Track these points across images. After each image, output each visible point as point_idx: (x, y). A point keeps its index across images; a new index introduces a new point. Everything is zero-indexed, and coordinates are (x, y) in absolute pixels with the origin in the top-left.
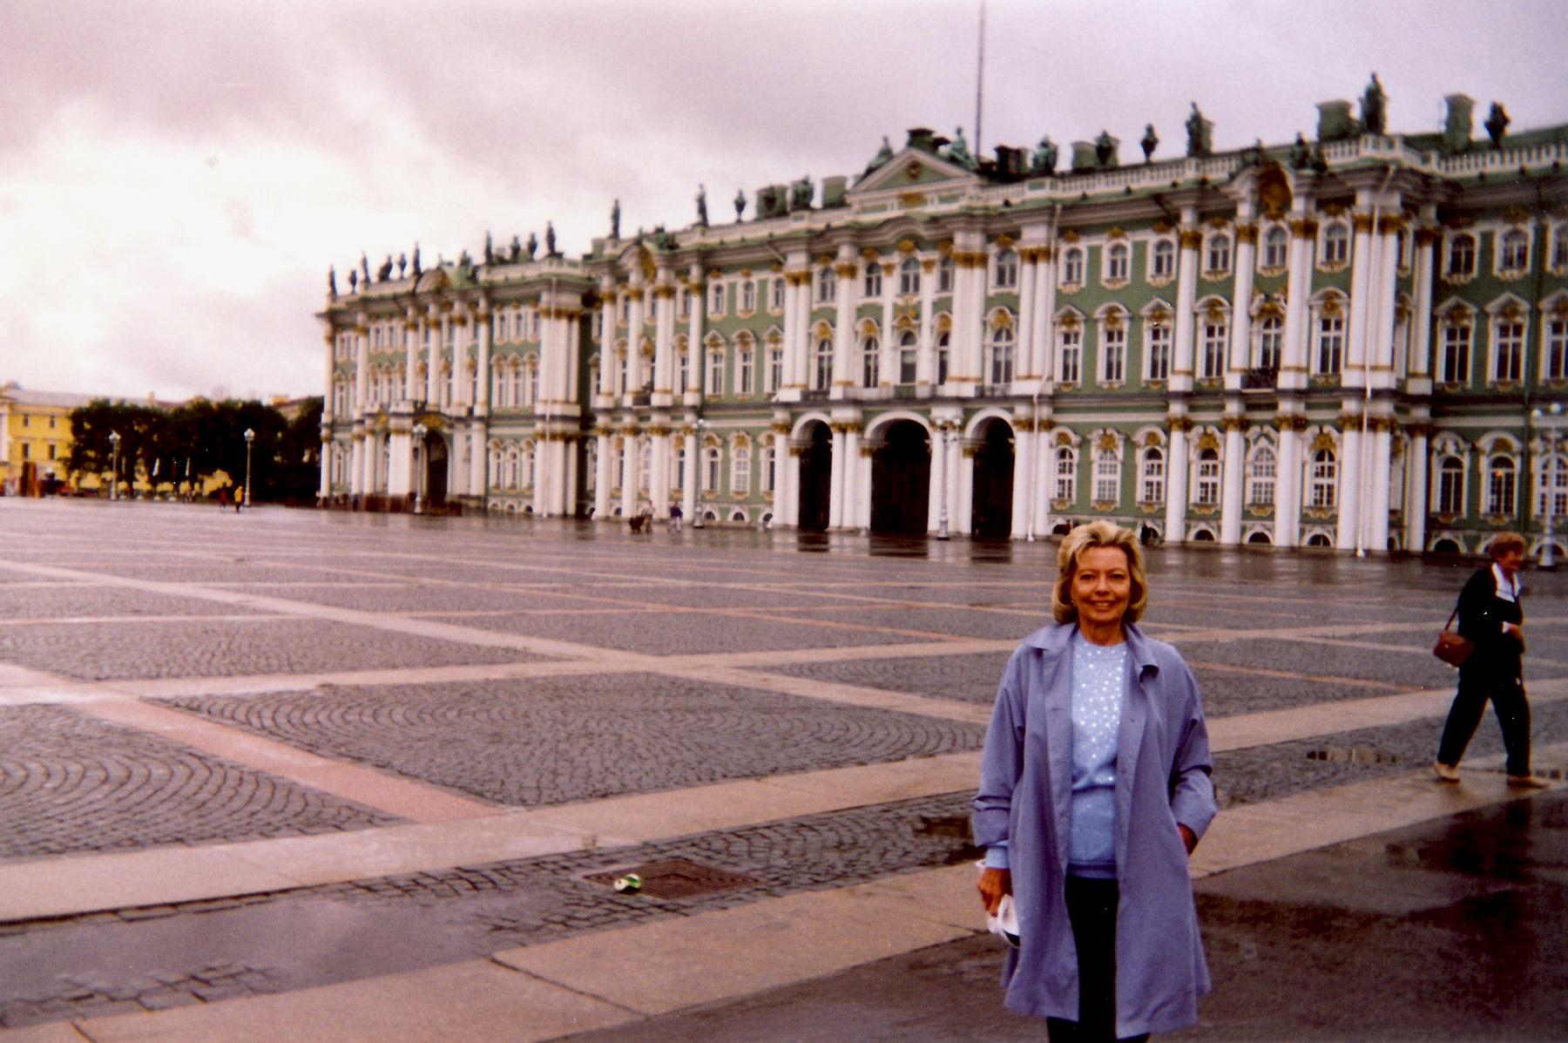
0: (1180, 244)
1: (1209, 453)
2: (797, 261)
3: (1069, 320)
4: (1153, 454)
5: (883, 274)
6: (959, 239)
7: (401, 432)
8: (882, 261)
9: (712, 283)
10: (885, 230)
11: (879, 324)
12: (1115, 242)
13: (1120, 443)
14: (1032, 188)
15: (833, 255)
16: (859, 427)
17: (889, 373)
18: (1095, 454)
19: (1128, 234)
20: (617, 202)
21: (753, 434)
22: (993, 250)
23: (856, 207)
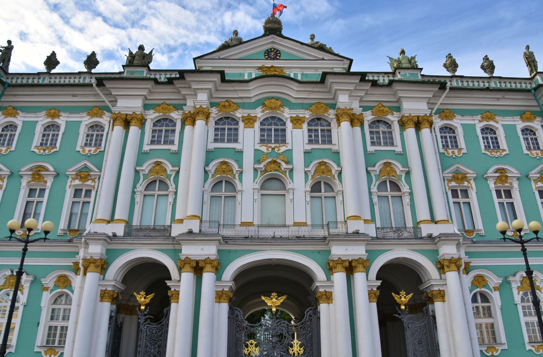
5: (241, 125)
6: (343, 100)
10: (252, 86)
11: (241, 166)
12: (485, 123)
18: (517, 298)
19: (497, 118)
22: (369, 117)
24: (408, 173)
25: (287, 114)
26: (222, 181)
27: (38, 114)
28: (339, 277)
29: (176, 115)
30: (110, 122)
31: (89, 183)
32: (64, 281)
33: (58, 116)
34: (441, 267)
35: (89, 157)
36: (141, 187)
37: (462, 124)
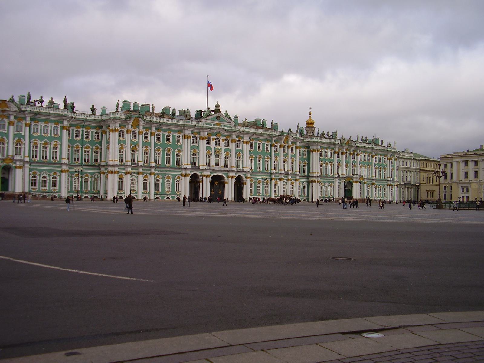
0: (271, 145)
1: (275, 185)
2: (188, 132)
3: (252, 157)
4: (267, 184)
7: (20, 168)
8: (212, 137)
9: (157, 133)
13: (262, 182)
14: (246, 128)
15: (199, 133)
16: (210, 176)
17: (212, 164)
19: (262, 142)
20: (118, 101)
21: (174, 176)
22: (237, 139)
23: (204, 122)
24: (243, 155)
25: (221, 138)
26: (208, 156)
27: (166, 132)
28: (230, 179)
29: (198, 136)
30: (183, 136)
31: (180, 153)
32: (179, 178)
33: (170, 133)
34: (247, 178)
35: (179, 146)
36: (191, 156)
37: (255, 143)
